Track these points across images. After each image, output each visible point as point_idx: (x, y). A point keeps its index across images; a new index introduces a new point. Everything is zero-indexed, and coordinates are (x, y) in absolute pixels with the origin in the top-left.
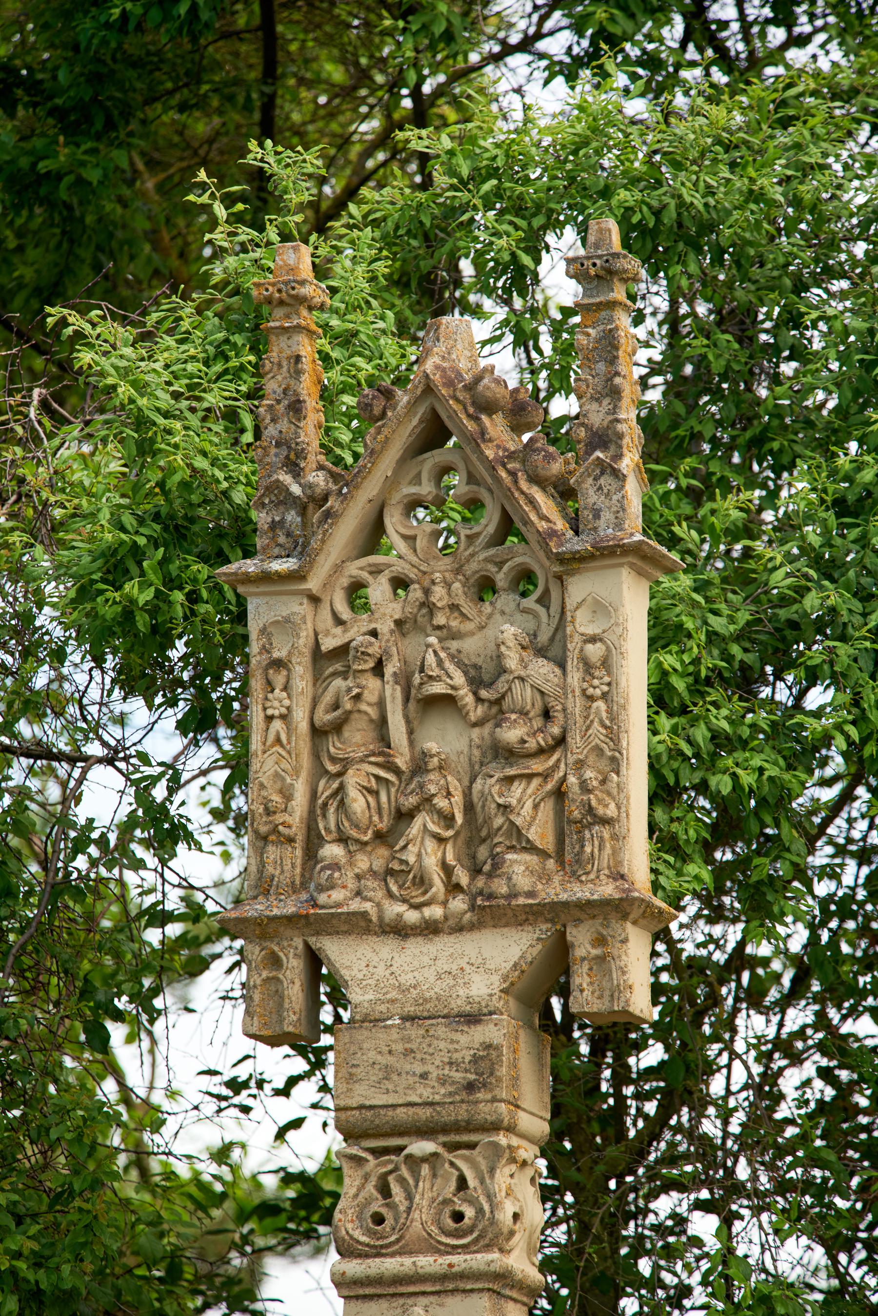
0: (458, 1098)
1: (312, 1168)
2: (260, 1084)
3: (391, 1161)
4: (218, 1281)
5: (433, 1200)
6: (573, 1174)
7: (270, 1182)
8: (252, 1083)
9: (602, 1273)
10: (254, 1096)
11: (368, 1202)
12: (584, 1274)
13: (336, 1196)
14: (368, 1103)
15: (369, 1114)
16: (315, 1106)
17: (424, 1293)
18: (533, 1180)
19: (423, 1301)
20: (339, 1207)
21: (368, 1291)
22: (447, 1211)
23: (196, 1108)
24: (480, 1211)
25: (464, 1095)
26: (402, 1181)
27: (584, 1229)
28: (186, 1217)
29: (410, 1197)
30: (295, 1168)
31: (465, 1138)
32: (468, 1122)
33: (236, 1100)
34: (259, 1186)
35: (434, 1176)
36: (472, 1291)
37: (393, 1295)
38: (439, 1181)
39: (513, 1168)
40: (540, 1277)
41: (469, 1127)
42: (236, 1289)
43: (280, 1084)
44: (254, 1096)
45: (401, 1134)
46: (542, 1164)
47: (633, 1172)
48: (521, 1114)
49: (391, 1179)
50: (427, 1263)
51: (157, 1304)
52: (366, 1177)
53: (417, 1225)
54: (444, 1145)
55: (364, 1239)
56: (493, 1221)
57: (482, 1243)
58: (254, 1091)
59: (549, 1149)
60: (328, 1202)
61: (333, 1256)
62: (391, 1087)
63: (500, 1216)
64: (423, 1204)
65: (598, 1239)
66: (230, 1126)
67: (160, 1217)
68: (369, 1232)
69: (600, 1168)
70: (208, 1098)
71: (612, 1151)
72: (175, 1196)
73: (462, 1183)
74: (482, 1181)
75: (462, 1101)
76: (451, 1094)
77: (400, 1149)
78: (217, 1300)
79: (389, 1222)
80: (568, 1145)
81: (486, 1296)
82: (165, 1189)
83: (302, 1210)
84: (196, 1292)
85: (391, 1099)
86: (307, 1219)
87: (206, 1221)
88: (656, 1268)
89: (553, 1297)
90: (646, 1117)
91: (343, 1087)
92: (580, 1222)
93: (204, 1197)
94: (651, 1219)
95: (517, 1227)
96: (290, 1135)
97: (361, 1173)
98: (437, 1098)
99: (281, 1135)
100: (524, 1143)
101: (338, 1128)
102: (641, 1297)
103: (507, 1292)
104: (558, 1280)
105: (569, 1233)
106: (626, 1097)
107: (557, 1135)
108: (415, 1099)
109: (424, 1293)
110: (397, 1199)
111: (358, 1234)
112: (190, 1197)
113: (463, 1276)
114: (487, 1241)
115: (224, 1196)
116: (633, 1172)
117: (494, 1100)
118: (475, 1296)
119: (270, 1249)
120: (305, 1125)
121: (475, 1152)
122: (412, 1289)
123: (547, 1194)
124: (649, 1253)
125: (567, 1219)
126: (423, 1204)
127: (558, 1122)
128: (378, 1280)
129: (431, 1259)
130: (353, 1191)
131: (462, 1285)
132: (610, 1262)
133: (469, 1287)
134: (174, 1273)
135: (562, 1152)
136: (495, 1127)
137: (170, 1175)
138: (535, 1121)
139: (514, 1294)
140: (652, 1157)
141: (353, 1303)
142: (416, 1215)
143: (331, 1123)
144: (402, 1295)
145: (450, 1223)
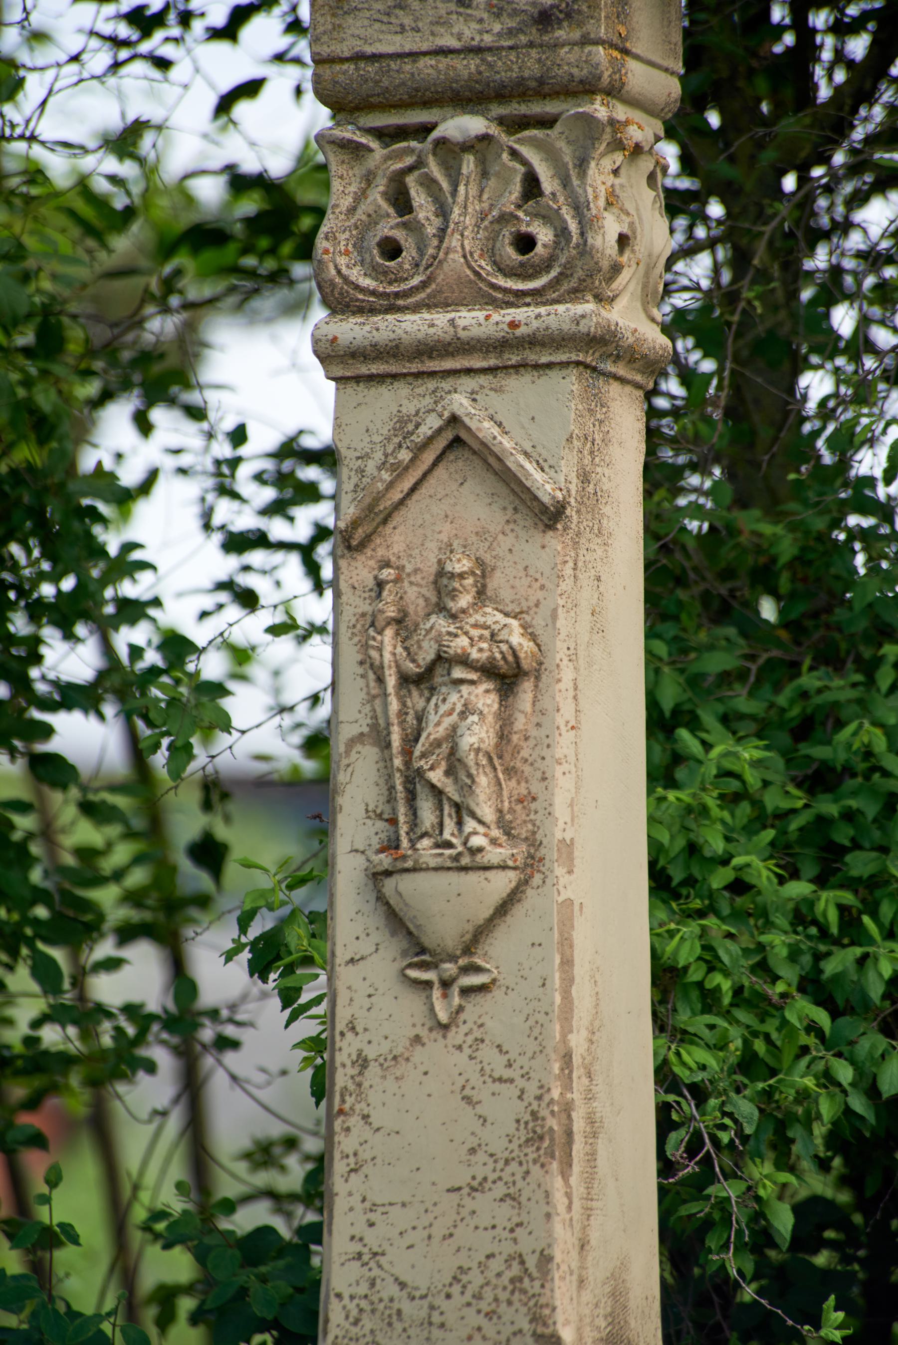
0: (523, 39)
1: (278, 165)
2: (186, 18)
3: (410, 151)
4: (126, 355)
5: (483, 215)
6: (723, 169)
7: (210, 191)
8: (172, 17)
9: (771, 333)
10: (176, 40)
11: (373, 220)
12: (739, 335)
13: (319, 212)
14: (369, 50)
15: (371, 69)
16: (280, 58)
17: (469, 371)
18: (651, 179)
19: (468, 383)
20: (324, 229)
21: (376, 368)
22: (507, 234)
23: (75, 58)
24: (562, 233)
25: (533, 34)
26: (429, 183)
27: (740, 261)
28: (64, 245)
29: (443, 212)
30: (250, 165)
31: (537, 108)
32: (541, 81)
33: (145, 47)
34: (189, 200)
35: (484, 174)
36: (550, 366)
37: (418, 375)
38: (492, 182)
39: (619, 158)
40: (664, 341)
41: (543, 89)
42: (156, 369)
43: (218, 17)
44: (176, 40)
45: (427, 104)
46: (670, 152)
47: (825, 160)
48: (632, 65)
49: (411, 181)
50: (473, 320)
51: (21, 392)
52: (369, 179)
53: (456, 257)
54: (501, 121)
55: (367, 282)
56: (584, 250)
57: (565, 286)
58: (175, 31)
59: (681, 126)
60: (306, 222)
61: (318, 313)
62: (407, 21)
63: (595, 240)
64: (466, 223)
65: (763, 276)
66: (136, 93)
67: (20, 246)
68: (375, 271)
69: (769, 156)
70: (94, 43)
71: (790, 125)
72: (44, 211)
73: (532, 186)
74: (565, 183)
75: (531, 45)
76: (511, 32)
77: (426, 129)
78: (126, 386)
79: (409, 254)
80: (714, 119)
81: (573, 374)
82: (29, 200)
83: (263, 237)
84: (87, 374)
85: (407, 43)
86: (272, 251)
87: (102, 255)
88: (864, 322)
89: (687, 376)
90: (850, 65)
91: (326, 23)
92: (736, 248)
93: (96, 216)
94: (855, 241)
95: (624, 259)
96: (242, 109)
97: (359, 171)
98: (488, 39)
99: (225, 105)
100: (637, 115)
101: (322, 96)
102: (837, 370)
103: (610, 367)
104: (697, 346)
105: (716, 269)
106: (814, 31)
107: (695, 100)
108: (451, 42)
109: (469, 371)
110: (421, 215)
111: (356, 274)
112: (72, 213)
113: (533, 341)
114: (574, 283)
115: (129, 213)
116: (825, 160)
117: (586, 41)
118: (555, 375)
119: (211, 302)
120: (266, 92)
121: (554, 133)
122: (449, 364)
123: (676, 204)
124: (850, 297)
125: (711, 244)
126: (466, 223)
127: (697, 78)
128: (392, 351)
129: (480, 315)
130: (346, 202)
131: (531, 357)
132: (782, 314)
133: (544, 360)
134: (50, 342)
135: (704, 129)
136: (587, 88)
137: (35, 174)
138: (656, 78)
139: (621, 370)
140: (859, 134)
141: (351, 388)
142: (454, 241)
143: (308, 86)
144: (432, 374)
145: (511, 254)
